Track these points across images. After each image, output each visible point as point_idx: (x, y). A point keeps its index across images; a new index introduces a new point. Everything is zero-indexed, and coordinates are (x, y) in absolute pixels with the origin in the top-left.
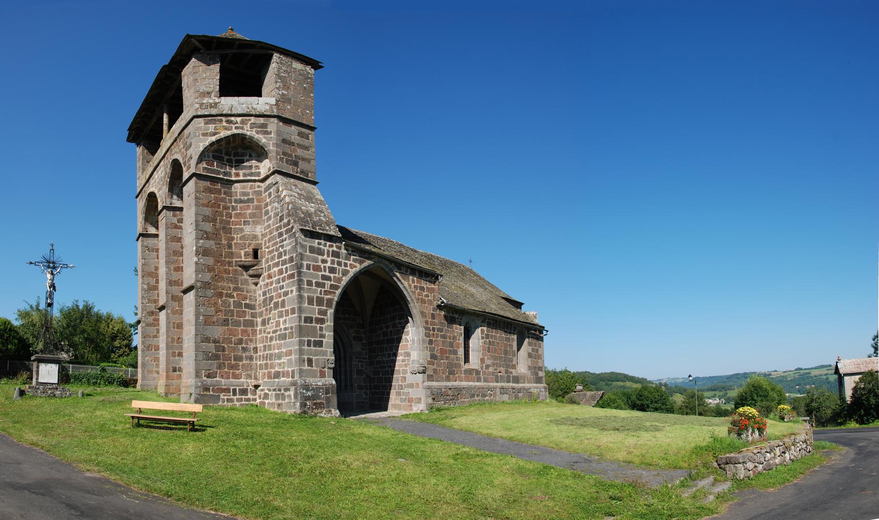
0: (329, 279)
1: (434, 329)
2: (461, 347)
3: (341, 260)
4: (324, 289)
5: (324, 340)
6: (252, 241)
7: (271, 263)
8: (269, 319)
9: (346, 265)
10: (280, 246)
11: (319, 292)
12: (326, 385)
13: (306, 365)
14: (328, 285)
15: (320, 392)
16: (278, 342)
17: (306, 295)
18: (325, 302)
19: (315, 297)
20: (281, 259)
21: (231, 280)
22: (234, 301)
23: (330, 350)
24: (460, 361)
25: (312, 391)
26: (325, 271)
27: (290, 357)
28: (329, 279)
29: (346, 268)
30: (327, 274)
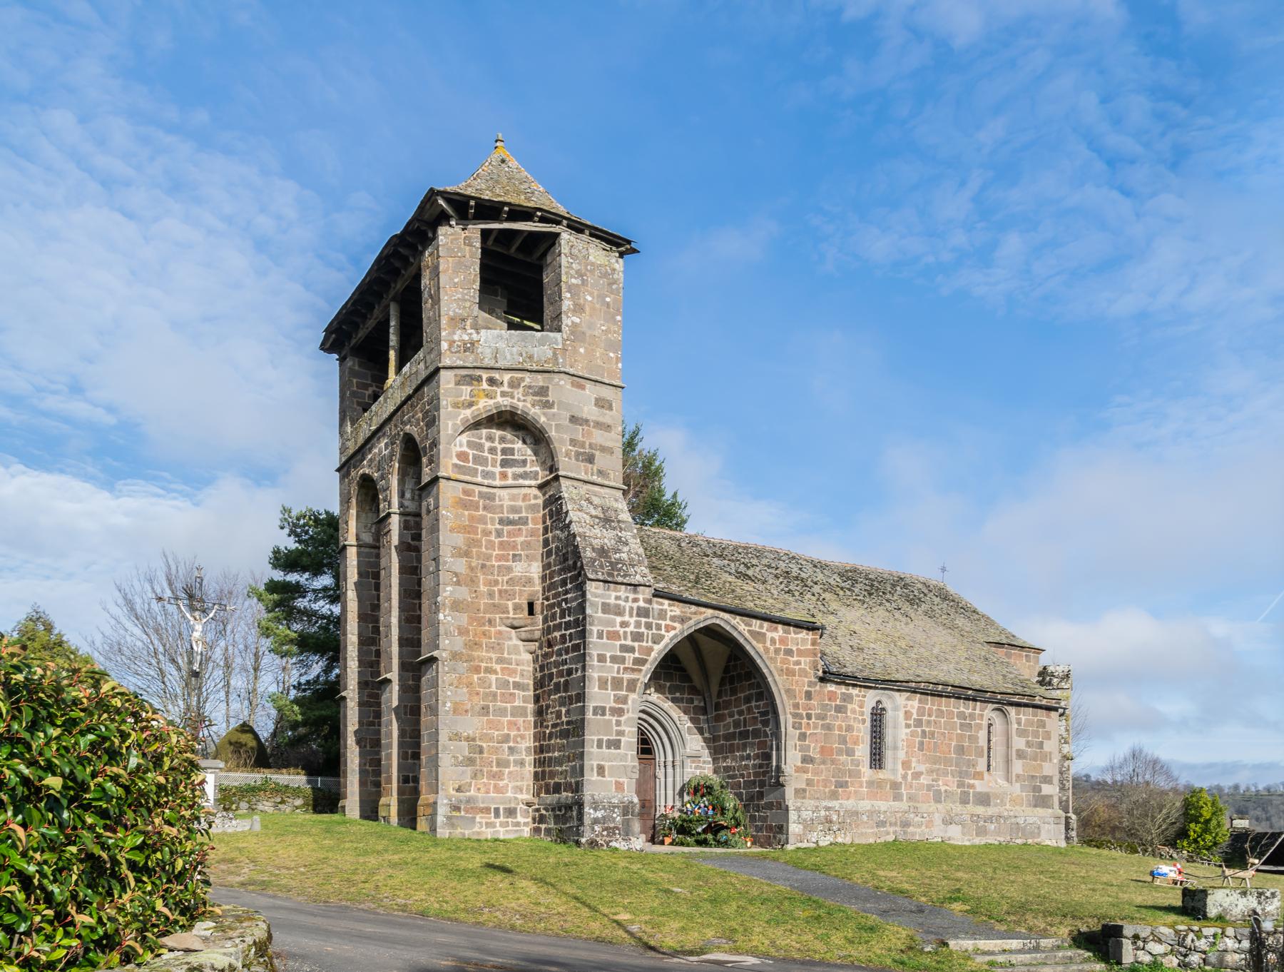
0: (632, 650)
1: (809, 717)
2: (863, 743)
3: (651, 620)
5: (623, 739)
6: (524, 586)
7: (551, 624)
8: (548, 707)
9: (659, 627)
10: (563, 600)
11: (616, 670)
13: (596, 775)
15: (614, 812)
16: (558, 741)
17: (596, 675)
18: (625, 684)
19: (610, 678)
20: (564, 620)
21: (493, 648)
22: (497, 679)
24: (858, 766)
25: (603, 811)
26: (625, 639)
27: (574, 763)
28: (632, 650)
29: (659, 632)
30: (629, 642)
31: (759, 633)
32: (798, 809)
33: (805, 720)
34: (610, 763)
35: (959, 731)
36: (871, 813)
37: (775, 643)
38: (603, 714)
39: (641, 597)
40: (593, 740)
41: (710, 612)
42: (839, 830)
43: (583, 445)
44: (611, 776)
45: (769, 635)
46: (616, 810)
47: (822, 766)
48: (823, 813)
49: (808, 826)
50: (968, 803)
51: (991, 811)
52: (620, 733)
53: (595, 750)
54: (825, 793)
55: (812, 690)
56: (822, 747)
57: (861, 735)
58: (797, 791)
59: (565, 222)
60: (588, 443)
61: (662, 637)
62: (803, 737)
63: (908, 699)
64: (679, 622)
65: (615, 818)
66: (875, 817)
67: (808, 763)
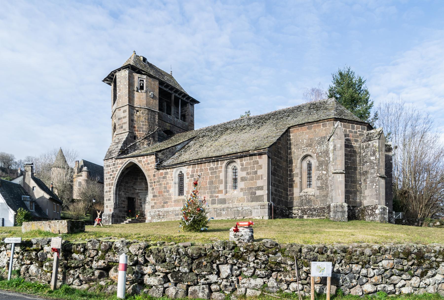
30: (111, 173)
32: (150, 212)
33: (154, 184)
35: (210, 175)
36: (173, 211)
45: (143, 160)
48: (157, 213)
49: (153, 217)
50: (215, 204)
51: (226, 205)
52: (110, 197)
62: (153, 189)
63: (187, 168)
66: (174, 212)
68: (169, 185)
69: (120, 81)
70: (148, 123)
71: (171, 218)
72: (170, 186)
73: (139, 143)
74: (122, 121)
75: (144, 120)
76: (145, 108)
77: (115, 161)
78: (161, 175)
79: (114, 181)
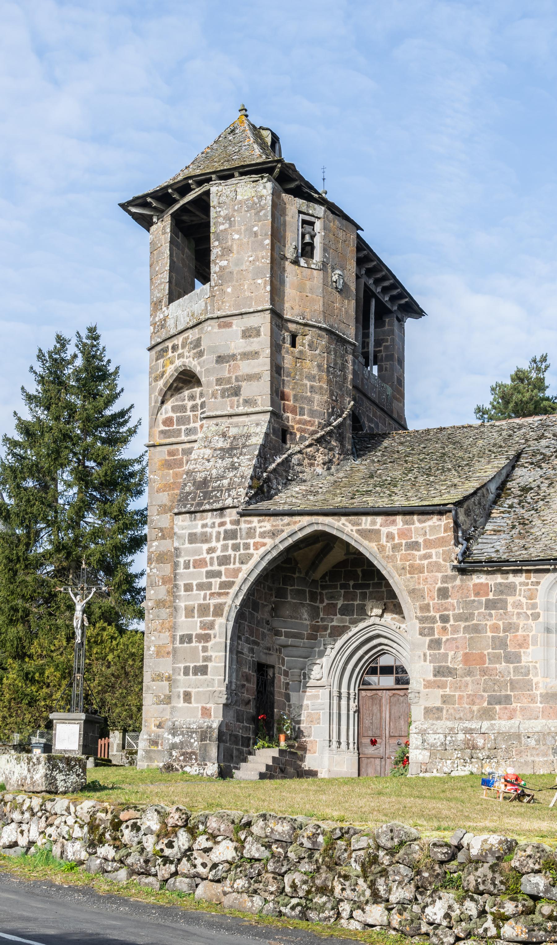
0: (218, 574)
1: (445, 619)
2: (535, 643)
3: (238, 541)
4: (210, 592)
5: (210, 665)
9: (247, 546)
11: (202, 597)
12: (202, 728)
14: (216, 585)
15: (192, 737)
18: (212, 609)
23: (219, 677)
25: (181, 737)
26: (212, 564)
28: (218, 574)
29: (248, 551)
30: (216, 567)
31: (370, 531)
32: (423, 733)
33: (439, 624)
34: (197, 690)
37: (393, 539)
38: (190, 641)
39: (227, 519)
40: (180, 668)
41: (306, 520)
42: (488, 757)
43: (229, 380)
44: (197, 702)
45: (384, 531)
46: (194, 735)
47: (468, 678)
52: (207, 659)
53: (181, 677)
54: (472, 712)
55: (449, 586)
56: (466, 654)
57: (531, 634)
58: (428, 711)
59: (214, 176)
60: (234, 377)
61: (250, 556)
64: (270, 537)
65: (192, 744)
67: (444, 676)
68: (520, 633)
69: (228, 218)
70: (329, 382)
71: (530, 759)
72: (525, 638)
73: (299, 456)
74: (237, 367)
75: (315, 371)
76: (320, 328)
77: (238, 522)
78: (477, 594)
79: (228, 600)
